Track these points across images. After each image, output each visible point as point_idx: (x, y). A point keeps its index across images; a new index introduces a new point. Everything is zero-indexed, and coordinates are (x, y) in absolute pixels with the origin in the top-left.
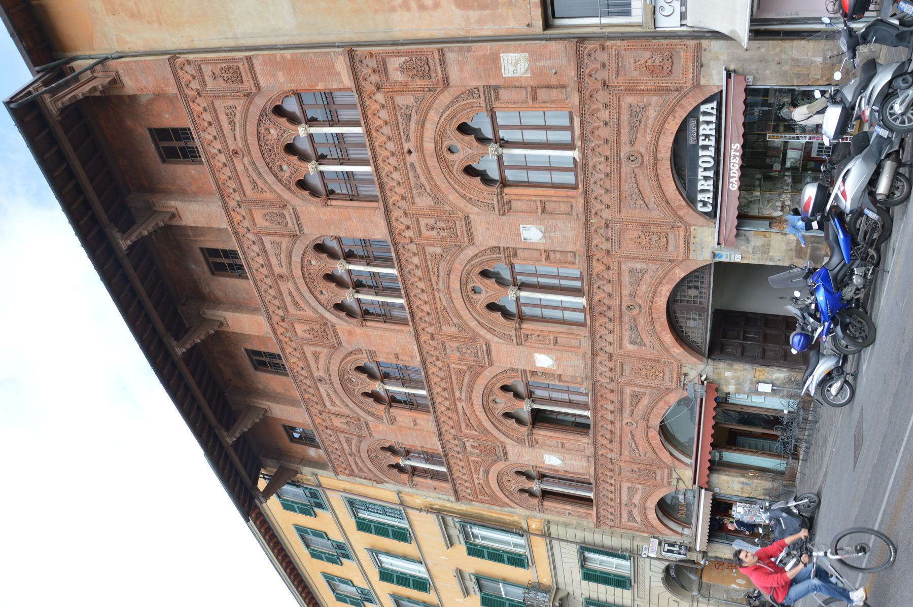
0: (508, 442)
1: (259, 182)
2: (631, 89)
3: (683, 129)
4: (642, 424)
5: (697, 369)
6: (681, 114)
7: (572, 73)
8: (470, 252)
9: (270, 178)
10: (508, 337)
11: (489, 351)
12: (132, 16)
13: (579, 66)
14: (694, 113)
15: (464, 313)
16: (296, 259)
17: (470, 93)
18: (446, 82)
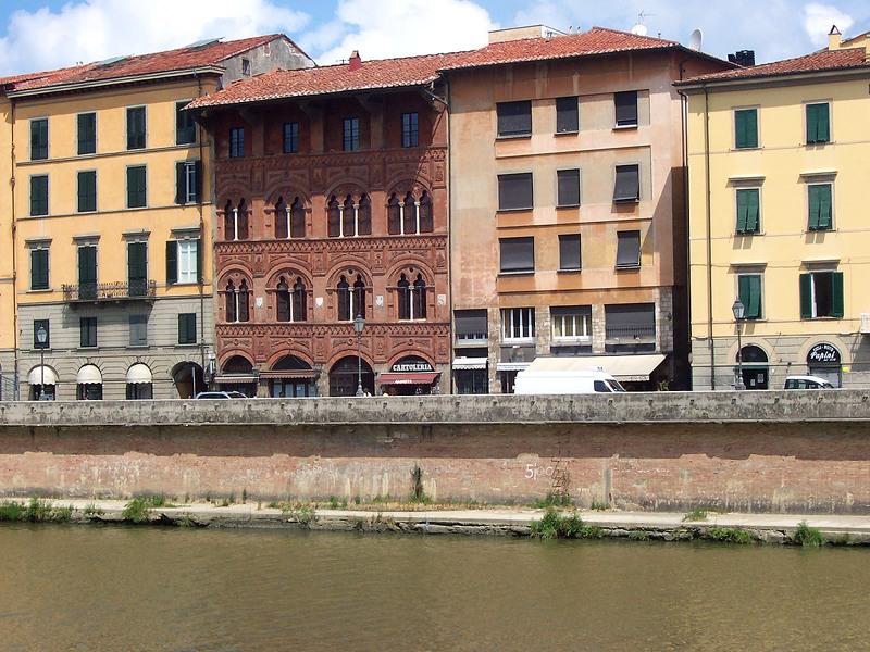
0: (267, 278)
1: (395, 173)
2: (434, 341)
3: (424, 360)
4: (292, 347)
5: (326, 369)
6: (427, 358)
7: (439, 321)
8: (370, 275)
9: (396, 180)
10: (329, 284)
11: (321, 276)
12: (465, 125)
13: (441, 324)
14: (428, 363)
15: (339, 265)
16: (358, 182)
17: (432, 281)
18: (435, 273)
